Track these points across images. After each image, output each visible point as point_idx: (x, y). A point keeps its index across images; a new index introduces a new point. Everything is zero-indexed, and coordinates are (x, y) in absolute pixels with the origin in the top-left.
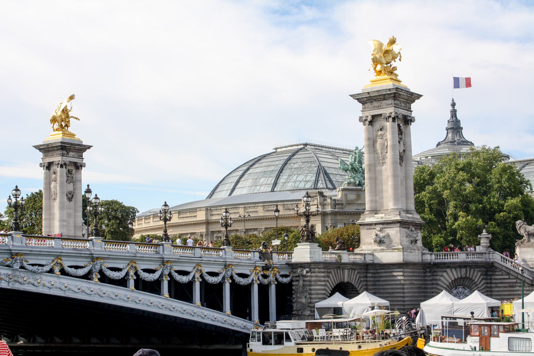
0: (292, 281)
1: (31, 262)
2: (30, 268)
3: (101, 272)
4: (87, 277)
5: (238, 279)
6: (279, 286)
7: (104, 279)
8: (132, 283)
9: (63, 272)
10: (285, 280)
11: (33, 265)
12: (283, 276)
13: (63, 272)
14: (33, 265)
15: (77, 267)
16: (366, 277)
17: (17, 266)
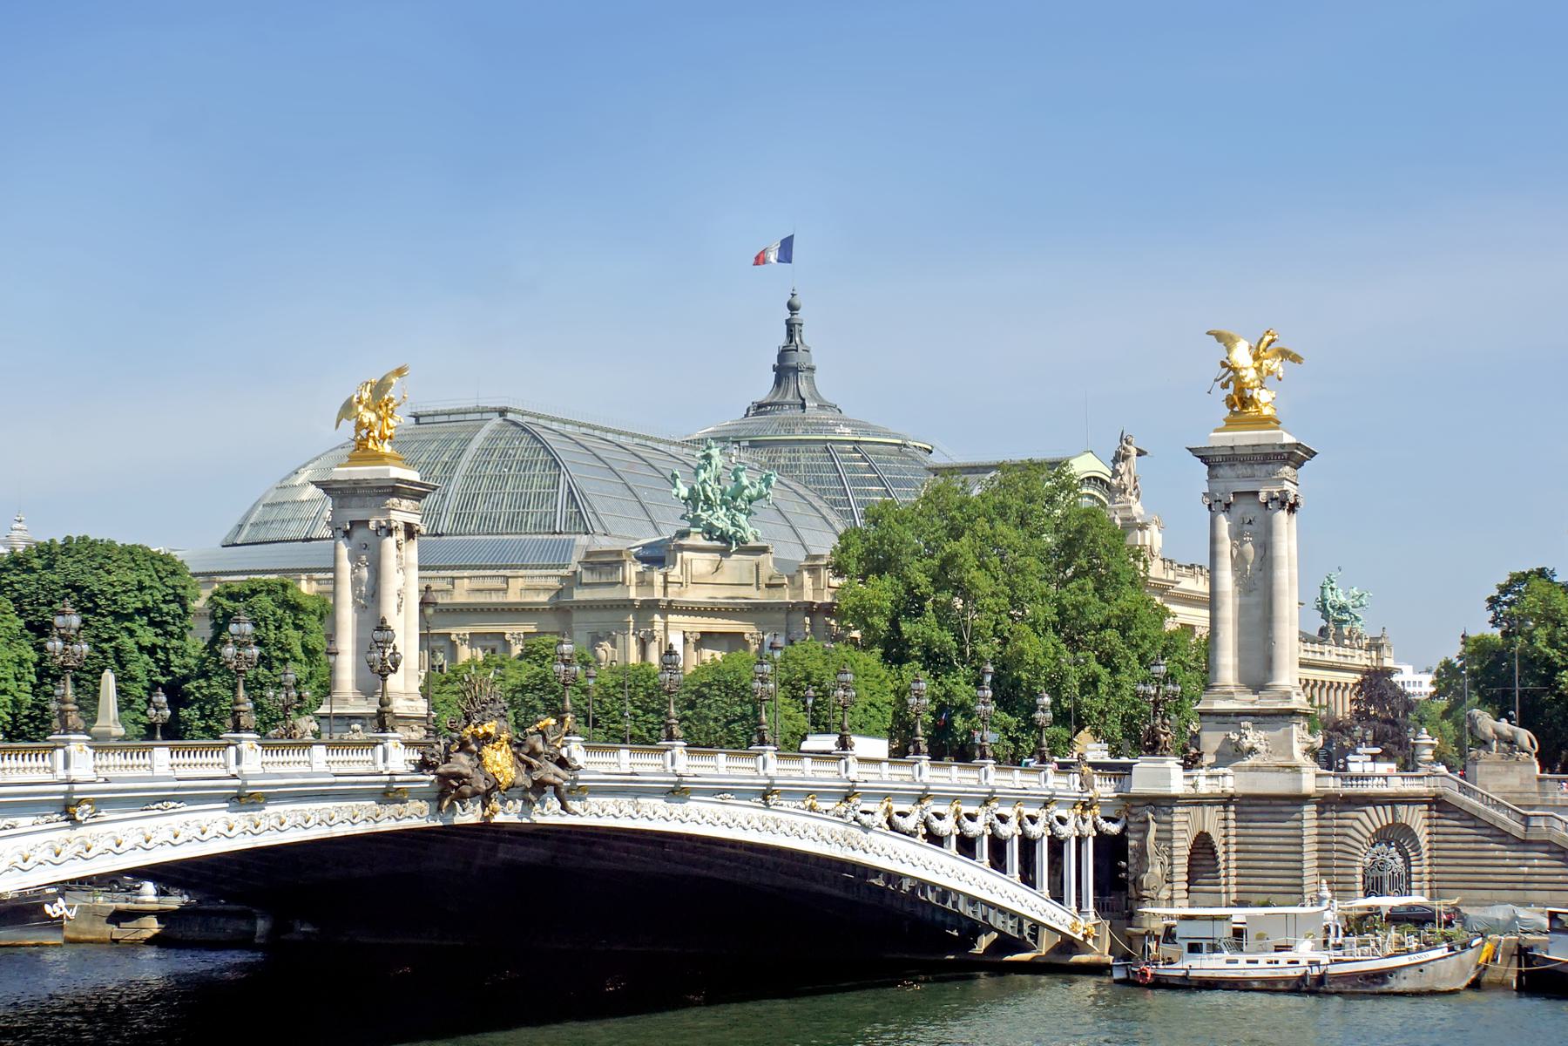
0: (1125, 829)
1: (865, 807)
2: (865, 819)
3: (926, 823)
4: (912, 834)
5: (1060, 828)
6: (1102, 839)
7: (935, 839)
8: (953, 839)
9: (893, 827)
10: (1114, 829)
11: (865, 812)
12: (1107, 819)
13: (893, 827)
14: (865, 812)
15: (904, 815)
16: (1225, 819)
17: (850, 817)
